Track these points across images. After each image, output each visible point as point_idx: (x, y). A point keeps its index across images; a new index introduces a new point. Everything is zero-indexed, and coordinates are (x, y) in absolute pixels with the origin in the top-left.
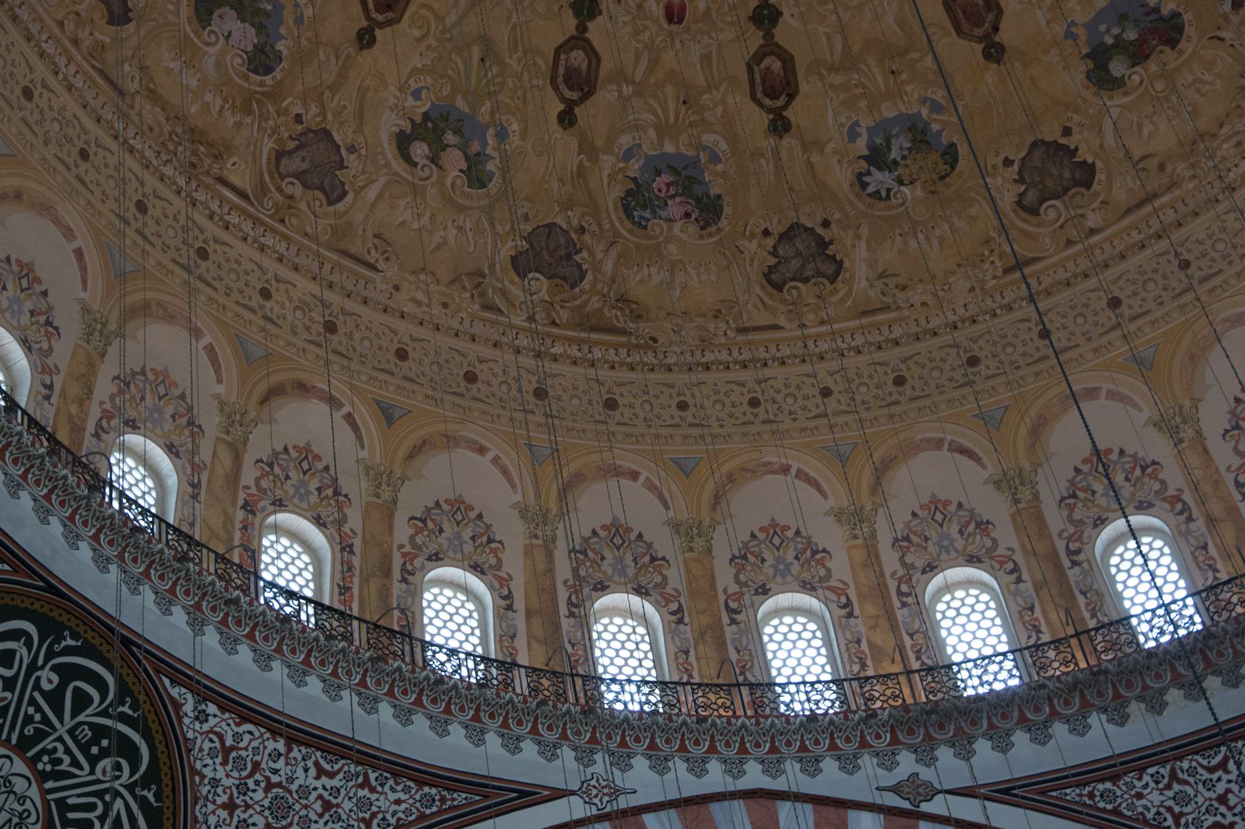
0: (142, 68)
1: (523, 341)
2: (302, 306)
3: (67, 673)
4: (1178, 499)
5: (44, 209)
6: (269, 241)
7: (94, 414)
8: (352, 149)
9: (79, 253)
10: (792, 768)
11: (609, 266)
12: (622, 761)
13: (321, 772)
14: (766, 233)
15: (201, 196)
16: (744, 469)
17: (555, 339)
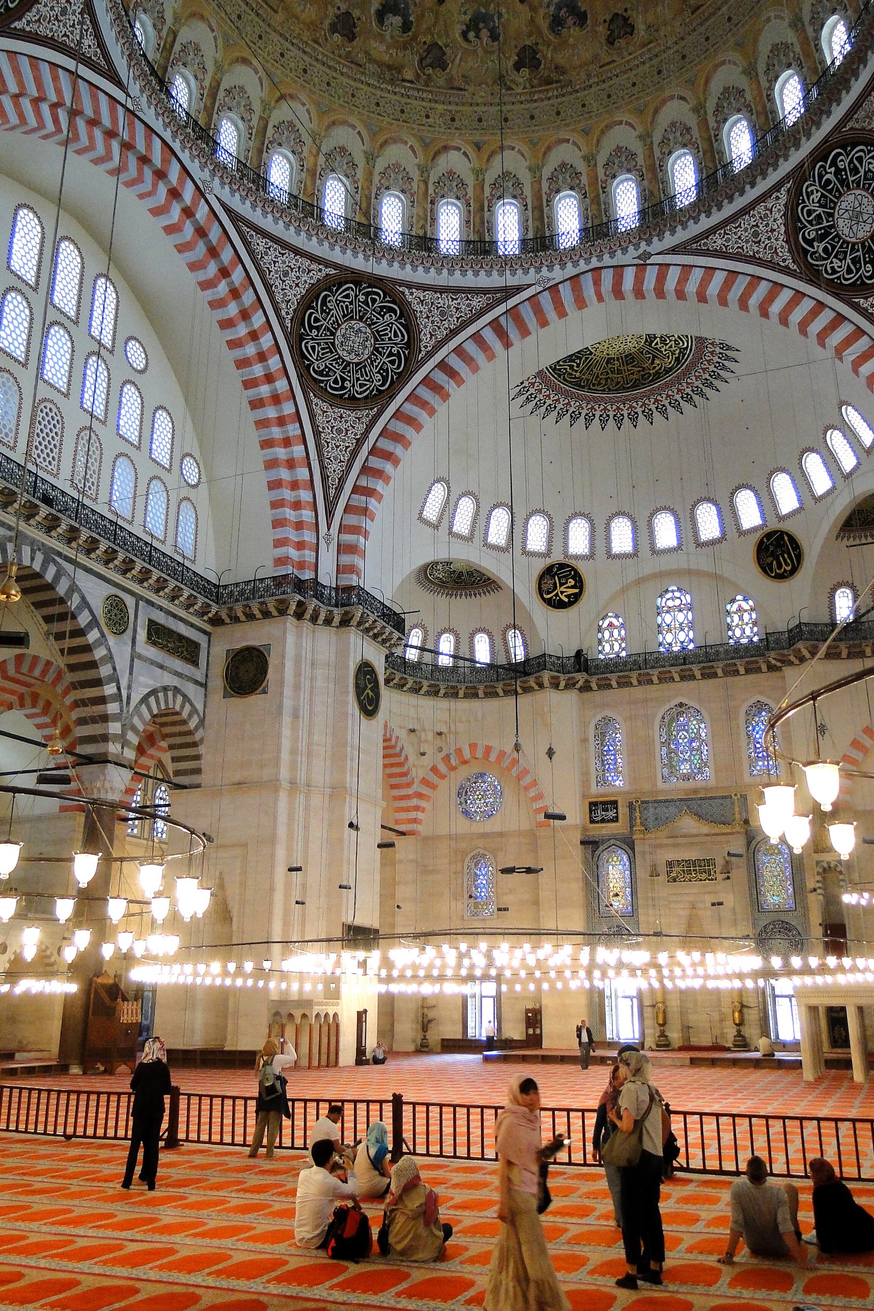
0: (366, 52)
1: (523, 98)
2: (441, 115)
3: (367, 294)
4: (749, 106)
5: (344, 123)
6: (425, 95)
7: (374, 190)
8: (446, 46)
9: (359, 133)
10: (606, 257)
11: (549, 55)
12: (550, 268)
13: (453, 299)
14: (605, 21)
15: (397, 90)
16: (606, 127)
17: (536, 92)
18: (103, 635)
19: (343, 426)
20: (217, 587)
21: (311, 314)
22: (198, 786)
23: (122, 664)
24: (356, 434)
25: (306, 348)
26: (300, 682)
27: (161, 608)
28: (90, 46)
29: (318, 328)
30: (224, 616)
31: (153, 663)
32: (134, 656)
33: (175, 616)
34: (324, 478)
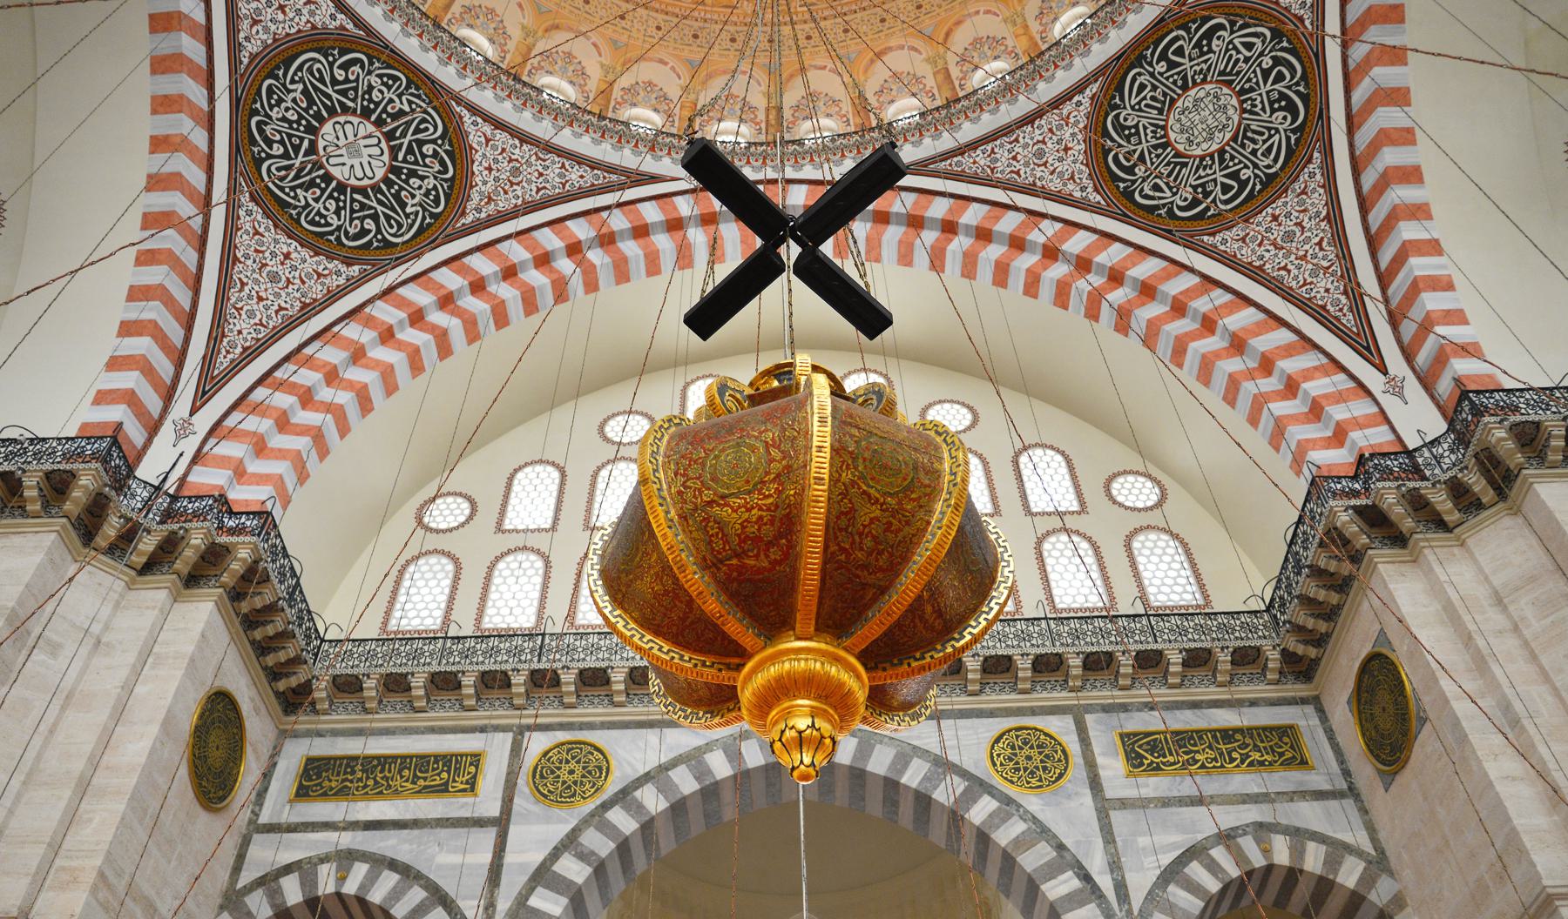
18: (1008, 801)
19: (1289, 225)
21: (1116, 158)
24: (1318, 214)
26: (1478, 651)
28: (582, 177)
30: (1300, 649)
31: (1166, 802)
32: (1104, 807)
34: (1320, 315)
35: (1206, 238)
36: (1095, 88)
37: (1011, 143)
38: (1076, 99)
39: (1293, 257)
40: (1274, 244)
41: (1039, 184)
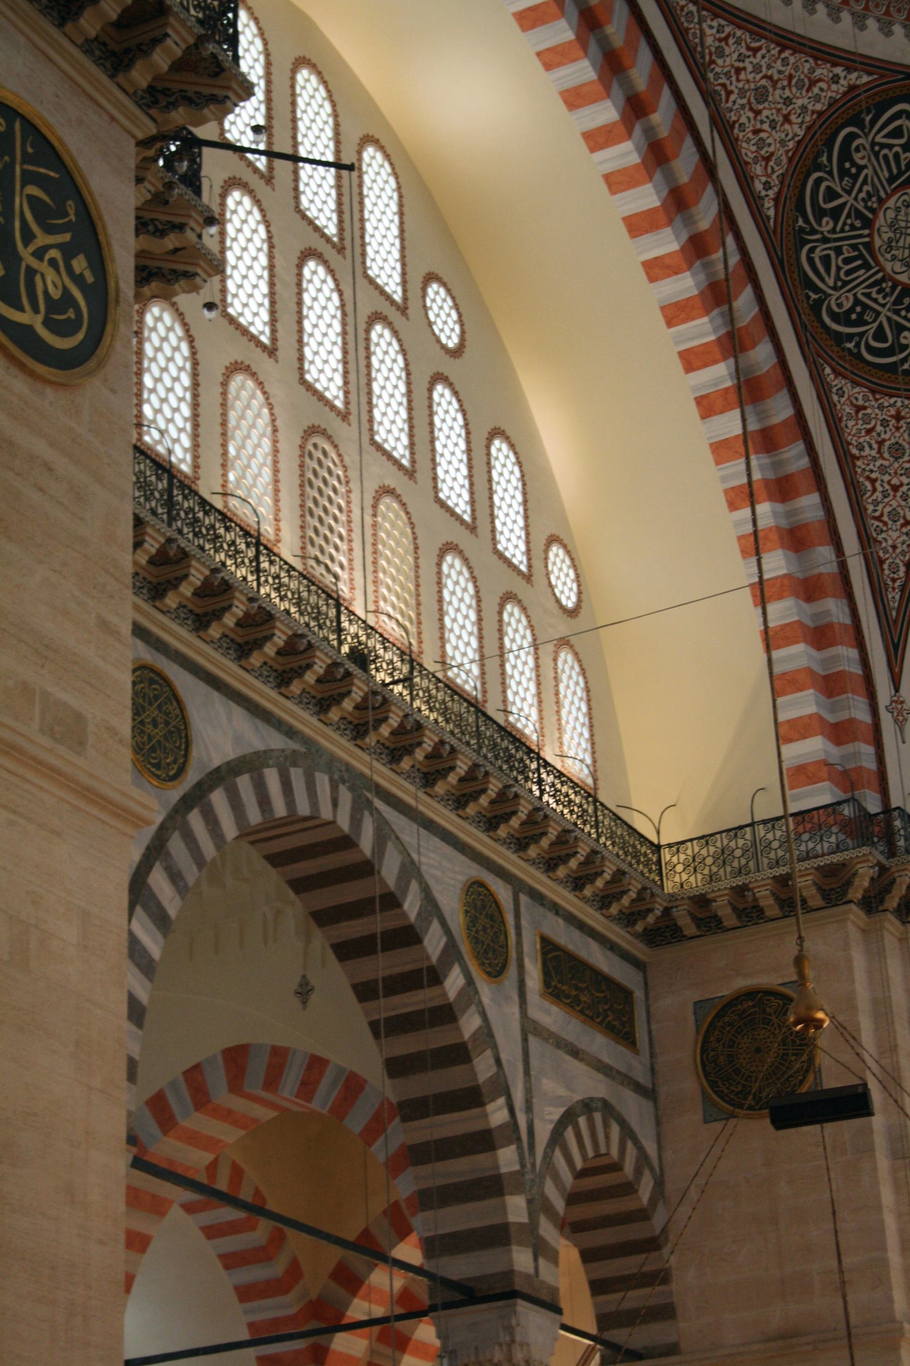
18: (470, 981)
20: (657, 848)
21: (819, 181)
22: (672, 1350)
23: (510, 1050)
25: (811, 261)
27: (556, 909)
29: (835, 214)
33: (582, 927)
34: (873, 566)
35: (828, 370)
36: (865, 79)
37: (749, 48)
38: (838, 70)
39: (886, 478)
40: (881, 443)
41: (736, 131)
